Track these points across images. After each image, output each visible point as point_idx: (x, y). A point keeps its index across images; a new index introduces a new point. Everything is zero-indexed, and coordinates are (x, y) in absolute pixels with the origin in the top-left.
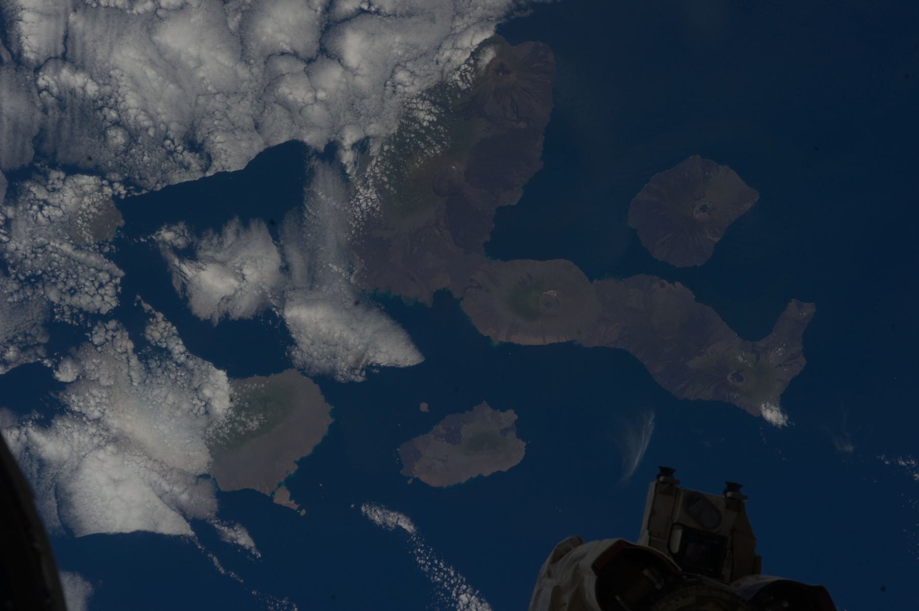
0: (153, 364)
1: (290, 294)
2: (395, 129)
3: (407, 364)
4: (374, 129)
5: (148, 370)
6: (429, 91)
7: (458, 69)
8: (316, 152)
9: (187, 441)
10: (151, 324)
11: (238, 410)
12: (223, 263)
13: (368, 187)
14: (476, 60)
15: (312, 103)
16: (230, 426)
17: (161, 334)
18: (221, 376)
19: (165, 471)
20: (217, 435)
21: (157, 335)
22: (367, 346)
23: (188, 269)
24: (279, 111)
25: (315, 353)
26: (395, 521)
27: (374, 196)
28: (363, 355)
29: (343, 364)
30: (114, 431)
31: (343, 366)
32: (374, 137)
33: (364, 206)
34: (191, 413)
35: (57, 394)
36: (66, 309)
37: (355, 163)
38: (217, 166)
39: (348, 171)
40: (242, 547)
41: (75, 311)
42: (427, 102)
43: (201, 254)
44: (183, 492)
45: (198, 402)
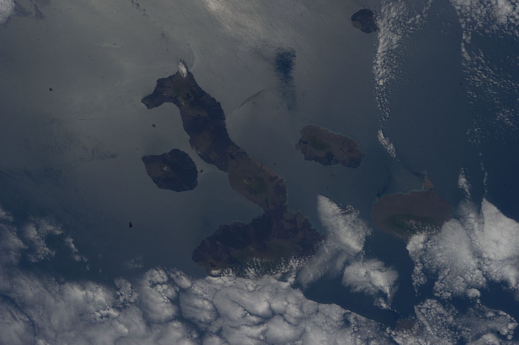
0: (434, 271)
1: (353, 254)
2: (266, 276)
3: (324, 198)
4: (274, 281)
5: (438, 270)
6: (244, 277)
7: (228, 276)
8: (302, 289)
9: (448, 235)
10: (420, 284)
11: (414, 232)
12: (371, 282)
13: (291, 266)
14: (220, 274)
15: (292, 304)
16: (424, 228)
17: (419, 278)
18: (410, 247)
19: (470, 232)
20: (433, 229)
21: (422, 279)
22: (337, 215)
23: (387, 290)
24: (305, 309)
25: (361, 228)
26: (384, 140)
27: (291, 261)
28: (343, 214)
29: (353, 216)
30: (477, 260)
31: (353, 216)
32: (276, 279)
33: (298, 261)
34: (436, 244)
35: (487, 288)
36: (450, 312)
37: (290, 276)
38: (344, 311)
39: (295, 276)
40: (466, 178)
41: (447, 309)
42: (247, 274)
43: (376, 291)
44: (471, 218)
45: (428, 245)
